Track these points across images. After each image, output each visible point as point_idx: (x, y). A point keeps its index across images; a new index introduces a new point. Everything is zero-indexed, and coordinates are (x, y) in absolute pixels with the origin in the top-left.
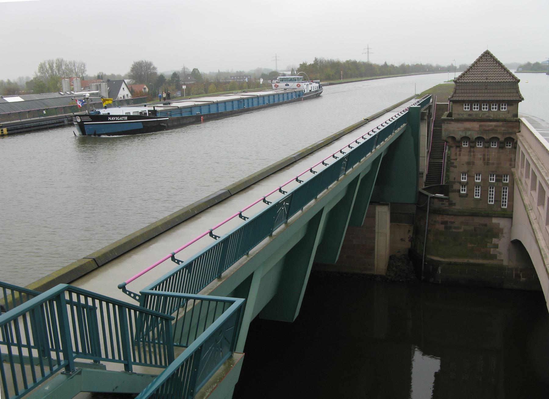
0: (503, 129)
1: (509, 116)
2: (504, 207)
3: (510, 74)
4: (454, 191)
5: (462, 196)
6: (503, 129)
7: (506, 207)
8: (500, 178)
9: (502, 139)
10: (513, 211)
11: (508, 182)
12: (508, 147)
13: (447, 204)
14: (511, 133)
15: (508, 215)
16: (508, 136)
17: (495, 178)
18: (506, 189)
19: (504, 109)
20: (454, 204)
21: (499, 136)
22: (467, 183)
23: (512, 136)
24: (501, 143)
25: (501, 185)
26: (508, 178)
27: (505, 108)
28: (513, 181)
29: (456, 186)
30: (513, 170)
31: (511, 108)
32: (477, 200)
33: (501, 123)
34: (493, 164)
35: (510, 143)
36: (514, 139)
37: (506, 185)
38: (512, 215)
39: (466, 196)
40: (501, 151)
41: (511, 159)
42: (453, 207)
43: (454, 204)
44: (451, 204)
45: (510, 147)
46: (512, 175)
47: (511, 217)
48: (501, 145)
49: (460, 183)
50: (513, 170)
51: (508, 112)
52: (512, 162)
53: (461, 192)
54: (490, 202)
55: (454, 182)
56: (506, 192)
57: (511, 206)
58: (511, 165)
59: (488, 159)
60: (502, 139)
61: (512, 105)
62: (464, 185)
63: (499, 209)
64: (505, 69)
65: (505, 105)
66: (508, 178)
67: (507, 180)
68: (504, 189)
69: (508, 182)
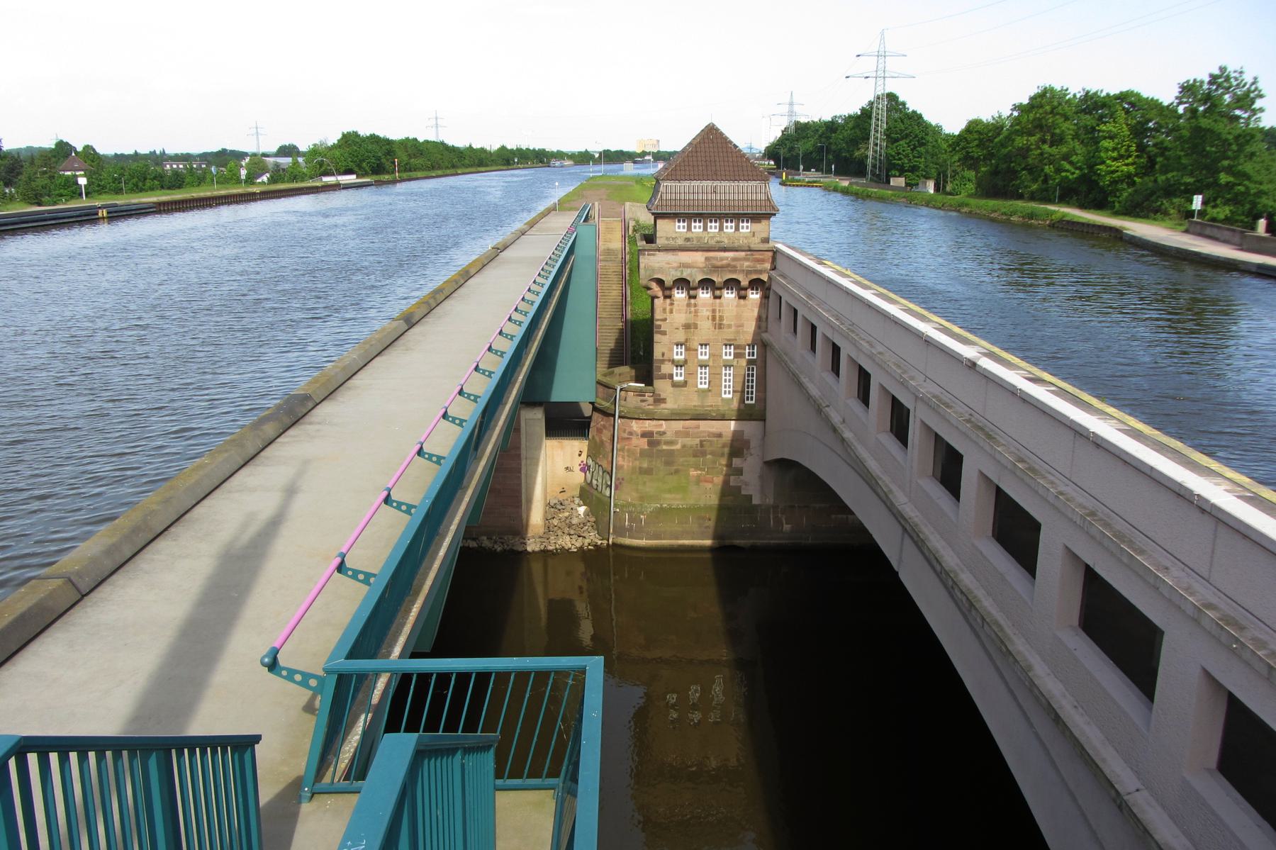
4: (663, 377)
5: (675, 385)
6: (746, 264)
9: (745, 283)
13: (651, 400)
20: (664, 401)
21: (740, 277)
22: (686, 361)
29: (666, 368)
31: (760, 227)
32: (703, 391)
33: (743, 254)
34: (729, 326)
39: (685, 384)
42: (663, 405)
43: (664, 401)
44: (659, 400)
49: (673, 361)
53: (675, 378)
55: (663, 361)
59: (721, 318)
60: (745, 283)
62: (679, 365)
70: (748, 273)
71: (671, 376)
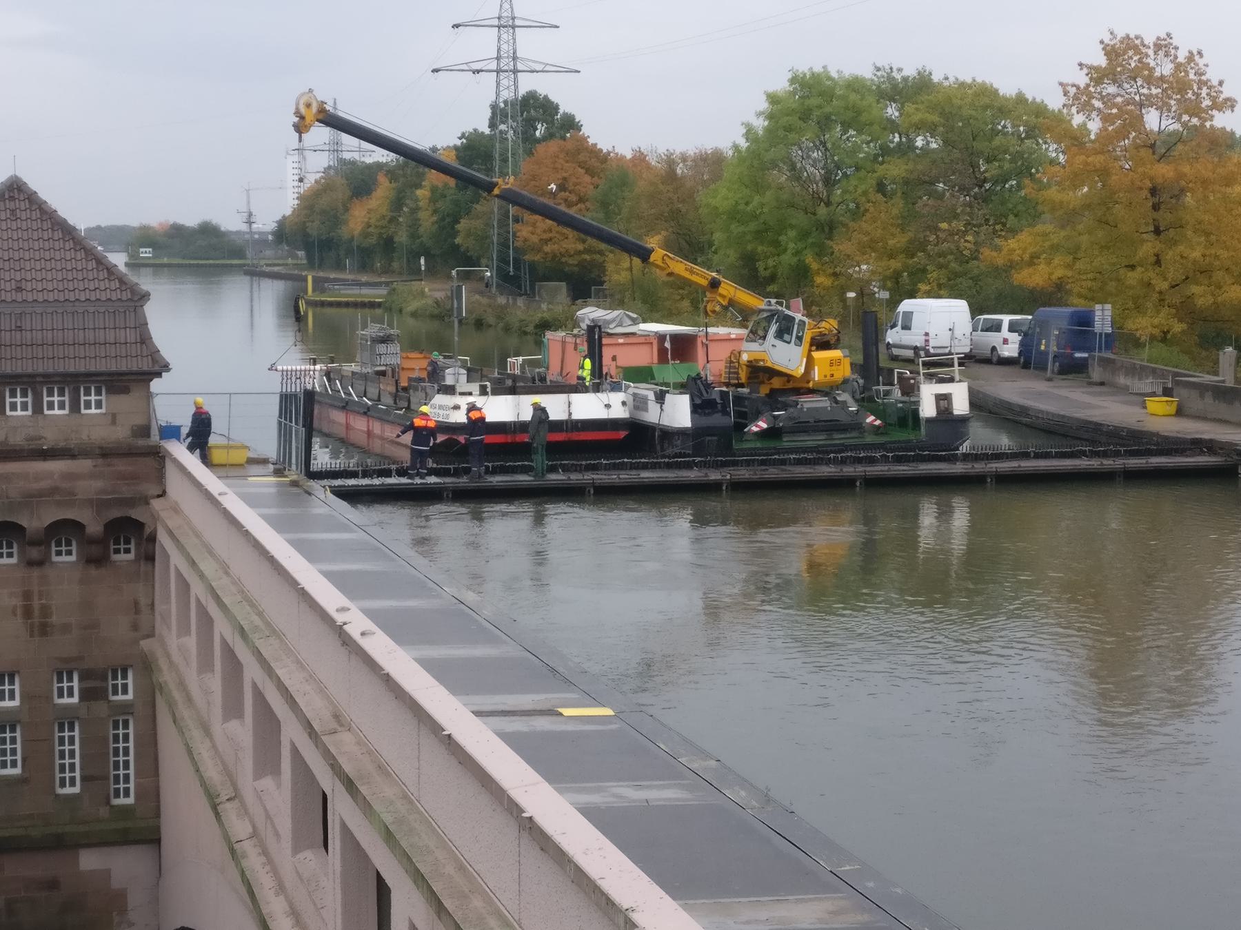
0: (98, 484)
1: (120, 433)
2: (122, 801)
3: (111, 270)
7: (130, 800)
8: (97, 684)
9: (94, 527)
10: (158, 814)
11: (130, 696)
12: (123, 557)
14: (130, 502)
15: (141, 830)
16: (116, 513)
18: (126, 726)
19: (95, 407)
23: (136, 514)
24: (92, 541)
25: (100, 708)
26: (130, 681)
27: (99, 405)
28: (151, 692)
30: (145, 644)
31: (123, 403)
33: (84, 465)
35: (127, 542)
36: (140, 526)
37: (126, 708)
38: (157, 829)
40: (93, 572)
41: (136, 603)
45: (131, 556)
46: (147, 667)
47: (150, 838)
48: (95, 550)
50: (145, 644)
51: (113, 418)
52: (141, 618)
57: (151, 795)
58: (135, 627)
60: (94, 527)
61: (125, 390)
63: (103, 812)
64: (90, 253)
65: (98, 393)
66: (130, 681)
67: (125, 691)
68: (116, 727)
69: (130, 696)
70: (100, 505)
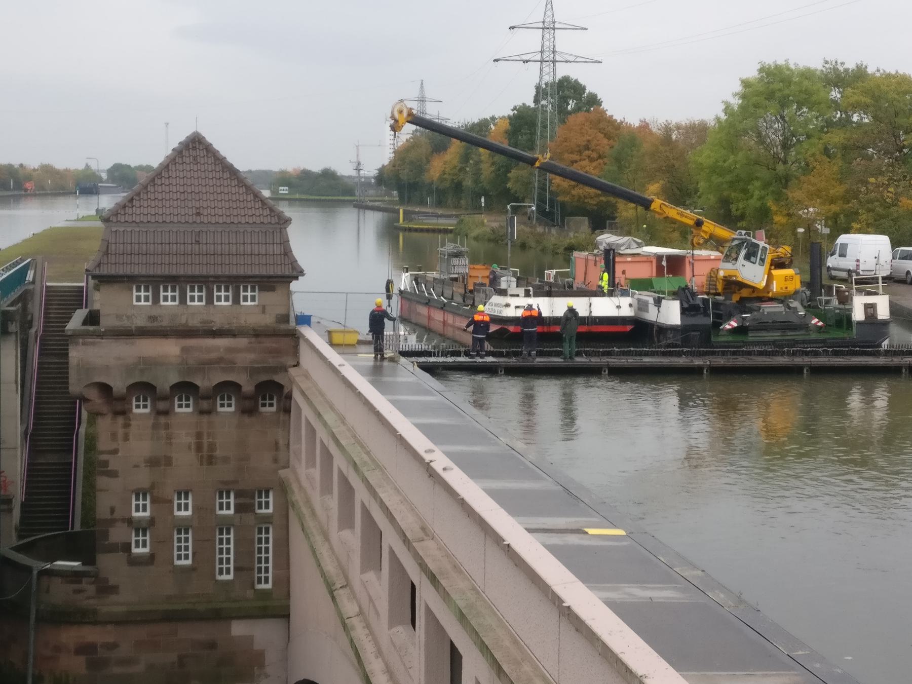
0: (252, 356)
1: (268, 320)
2: (263, 586)
3: (263, 201)
4: (113, 549)
5: (135, 561)
6: (252, 356)
7: (269, 586)
8: (247, 501)
9: (248, 387)
10: (288, 596)
11: (271, 510)
13: (91, 589)
15: (277, 608)
16: (264, 378)
17: (232, 500)
18: (267, 532)
19: (250, 300)
20: (114, 589)
22: (152, 521)
23: (278, 378)
24: (247, 398)
25: (249, 518)
26: (271, 499)
28: (286, 506)
29: (117, 534)
31: (270, 298)
32: (183, 569)
33: (242, 342)
34: (226, 460)
35: (271, 398)
36: (280, 387)
37: (267, 519)
38: (288, 607)
39: (150, 559)
40: (247, 420)
41: (277, 443)
42: (113, 598)
43: (114, 589)
44: (106, 589)
45: (274, 409)
46: (283, 489)
48: (248, 404)
49: (130, 521)
51: (263, 309)
52: (279, 453)
53: (135, 550)
54: (221, 573)
55: (112, 522)
56: (267, 541)
57: (284, 582)
58: (276, 460)
59: (212, 447)
60: (248, 387)
61: (272, 289)
62: (140, 527)
63: (250, 594)
64: (248, 189)
65: (253, 290)
66: (271, 499)
67: (267, 507)
68: (260, 532)
69: (271, 510)
70: (253, 371)
71: (127, 547)
